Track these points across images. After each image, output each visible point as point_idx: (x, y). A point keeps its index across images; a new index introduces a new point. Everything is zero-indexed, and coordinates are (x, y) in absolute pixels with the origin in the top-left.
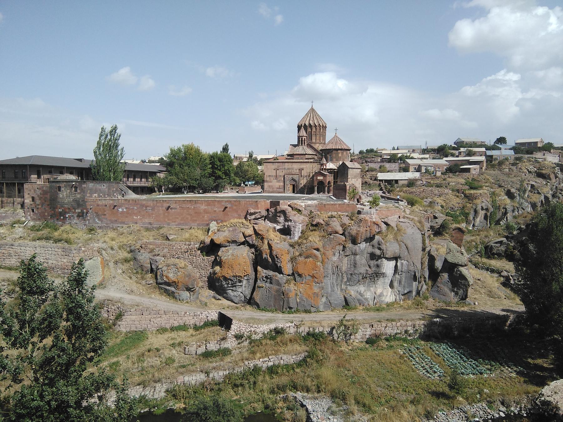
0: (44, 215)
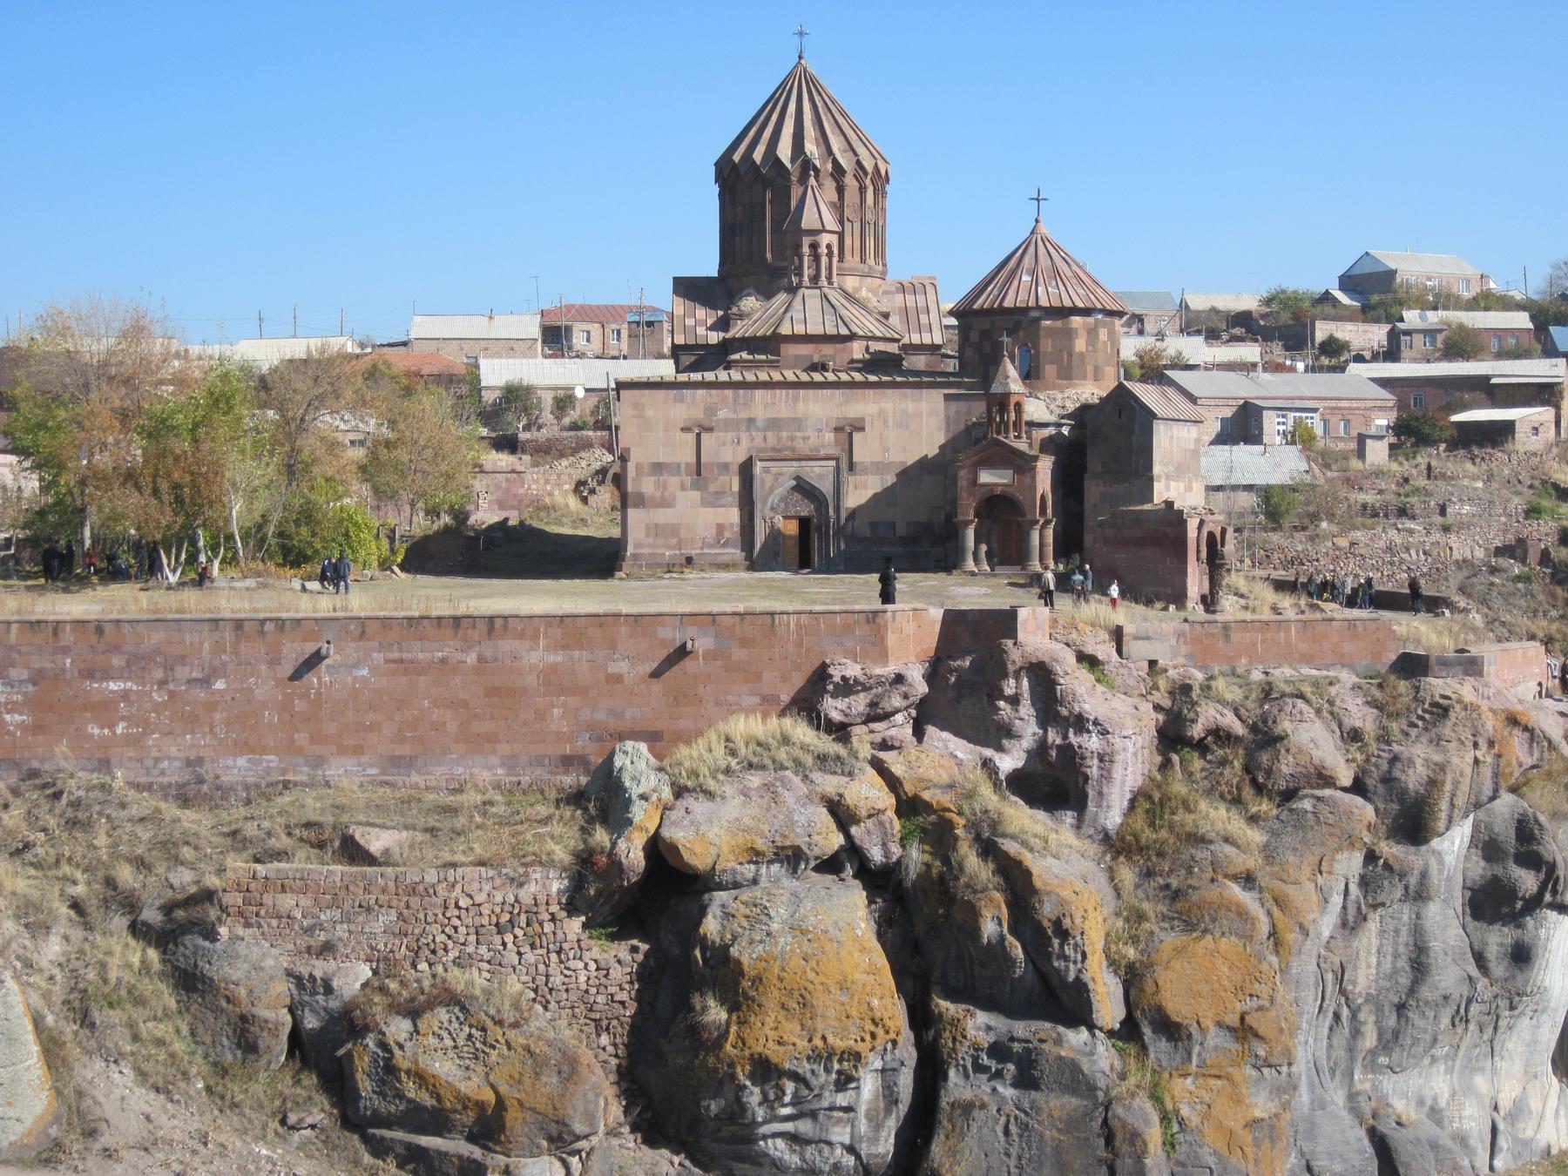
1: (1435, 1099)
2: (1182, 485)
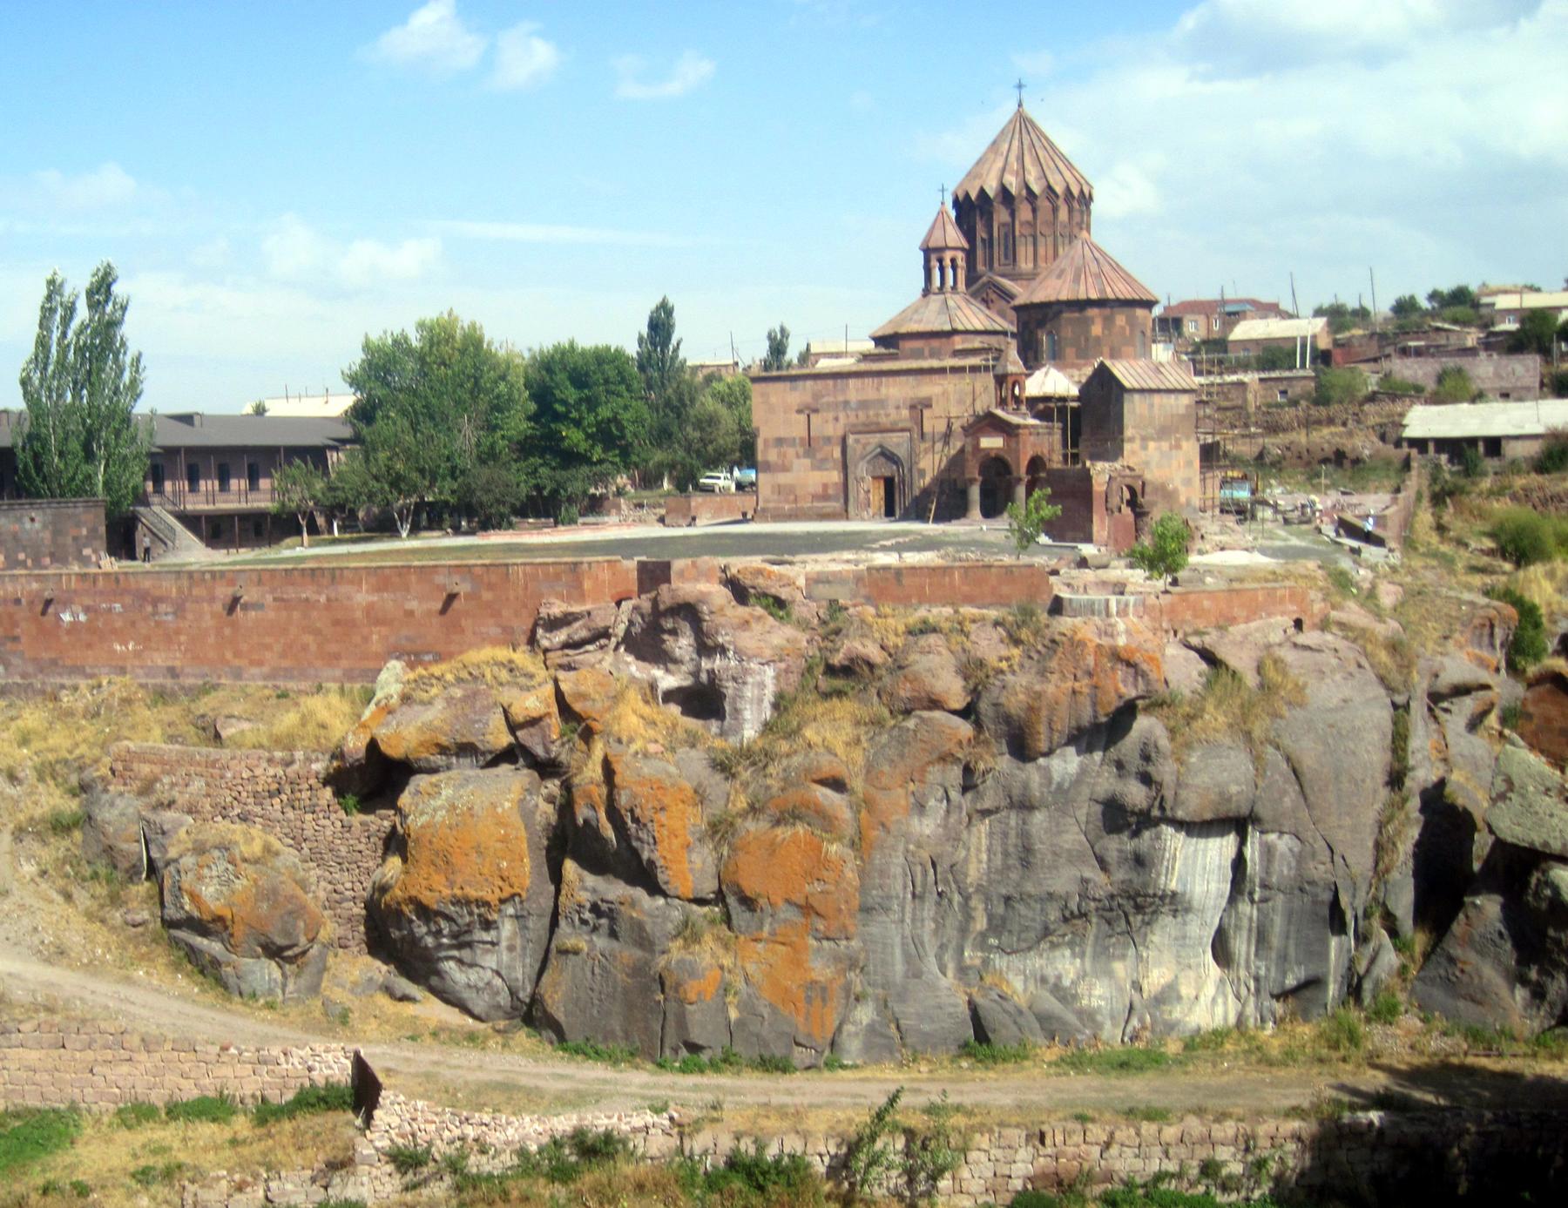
1: (1059, 977)
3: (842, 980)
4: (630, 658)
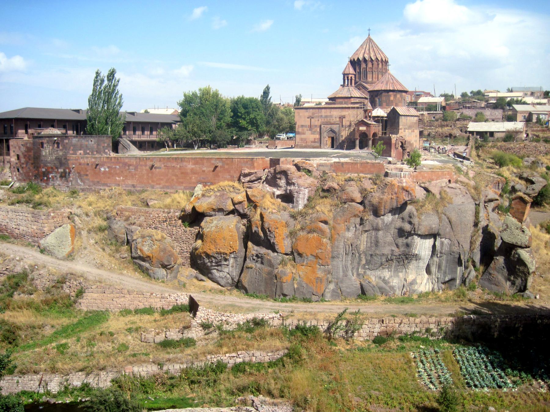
0: (29, 176)
1: (384, 277)
2: (410, 131)
3: (326, 277)
4: (267, 186)
